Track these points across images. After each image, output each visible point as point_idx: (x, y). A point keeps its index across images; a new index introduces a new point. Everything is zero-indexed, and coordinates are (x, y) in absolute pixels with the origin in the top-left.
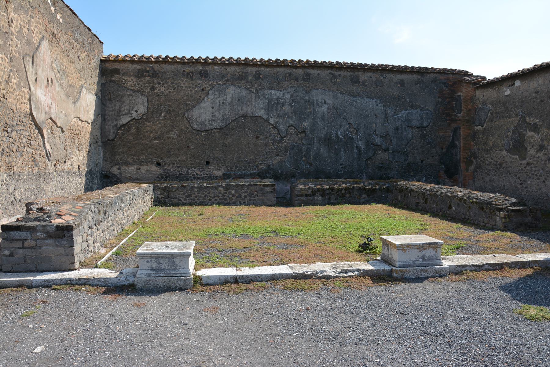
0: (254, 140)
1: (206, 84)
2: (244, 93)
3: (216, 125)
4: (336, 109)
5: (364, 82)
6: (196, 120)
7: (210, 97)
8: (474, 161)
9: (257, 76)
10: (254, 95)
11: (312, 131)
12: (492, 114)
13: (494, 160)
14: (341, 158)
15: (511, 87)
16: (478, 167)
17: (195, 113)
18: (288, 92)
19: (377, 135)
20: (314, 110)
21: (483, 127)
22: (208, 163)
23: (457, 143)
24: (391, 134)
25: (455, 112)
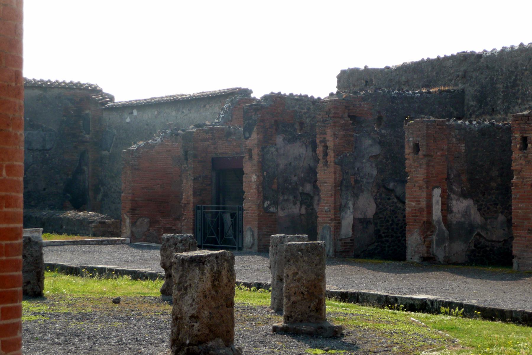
8: (102, 188)
12: (116, 139)
13: (118, 188)
15: (130, 115)
16: (105, 195)
21: (109, 152)
23: (85, 168)
25: (82, 132)
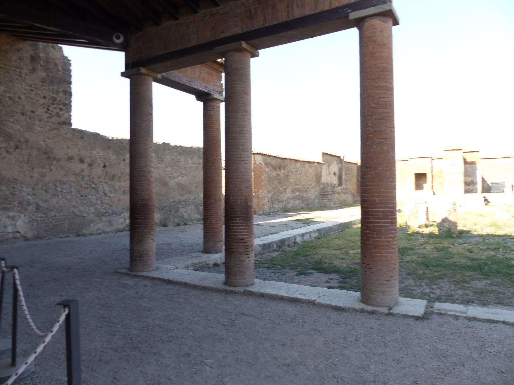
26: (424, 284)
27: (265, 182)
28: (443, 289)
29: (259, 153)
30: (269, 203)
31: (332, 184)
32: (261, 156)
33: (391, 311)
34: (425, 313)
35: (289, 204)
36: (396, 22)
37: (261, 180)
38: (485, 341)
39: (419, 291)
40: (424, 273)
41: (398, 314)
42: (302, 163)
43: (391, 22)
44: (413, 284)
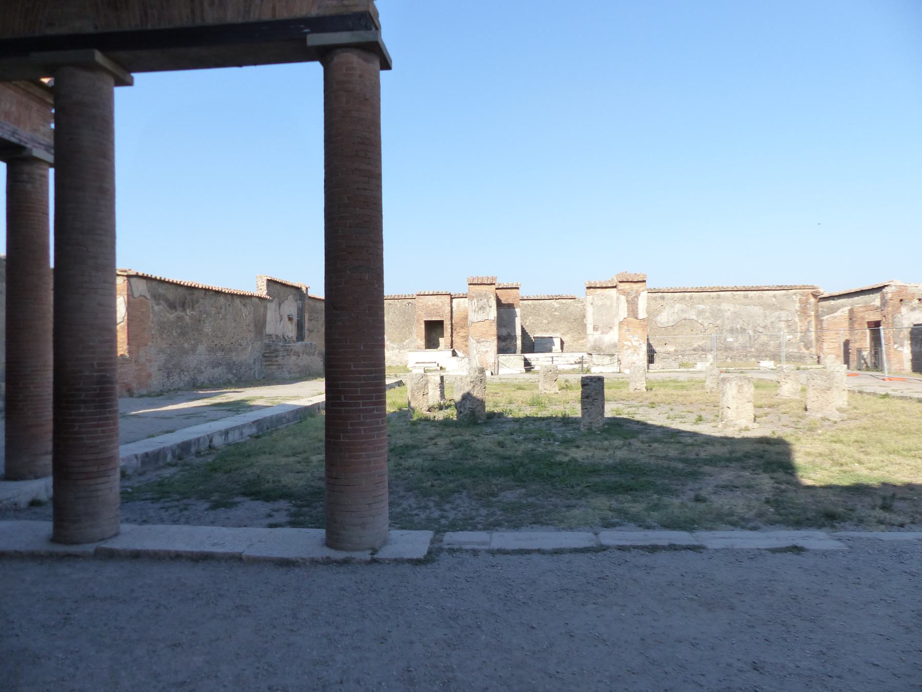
0: (691, 332)
1: (664, 303)
2: (684, 307)
3: (670, 324)
4: (735, 313)
5: (752, 297)
6: (660, 323)
7: (666, 310)
9: (691, 298)
10: (689, 308)
11: (722, 326)
14: (739, 340)
17: (659, 318)
18: (708, 306)
19: (760, 326)
20: (723, 315)
22: (666, 344)
24: (769, 326)
26: (431, 504)
27: (153, 332)
28: (460, 509)
29: (140, 274)
30: (161, 372)
31: (286, 338)
32: (144, 281)
33: (375, 556)
34: (429, 553)
35: (203, 374)
36: (386, 65)
37: (145, 329)
38: (513, 584)
39: (423, 516)
40: (432, 486)
41: (387, 559)
42: (229, 297)
43: (377, 64)
44: (414, 506)
